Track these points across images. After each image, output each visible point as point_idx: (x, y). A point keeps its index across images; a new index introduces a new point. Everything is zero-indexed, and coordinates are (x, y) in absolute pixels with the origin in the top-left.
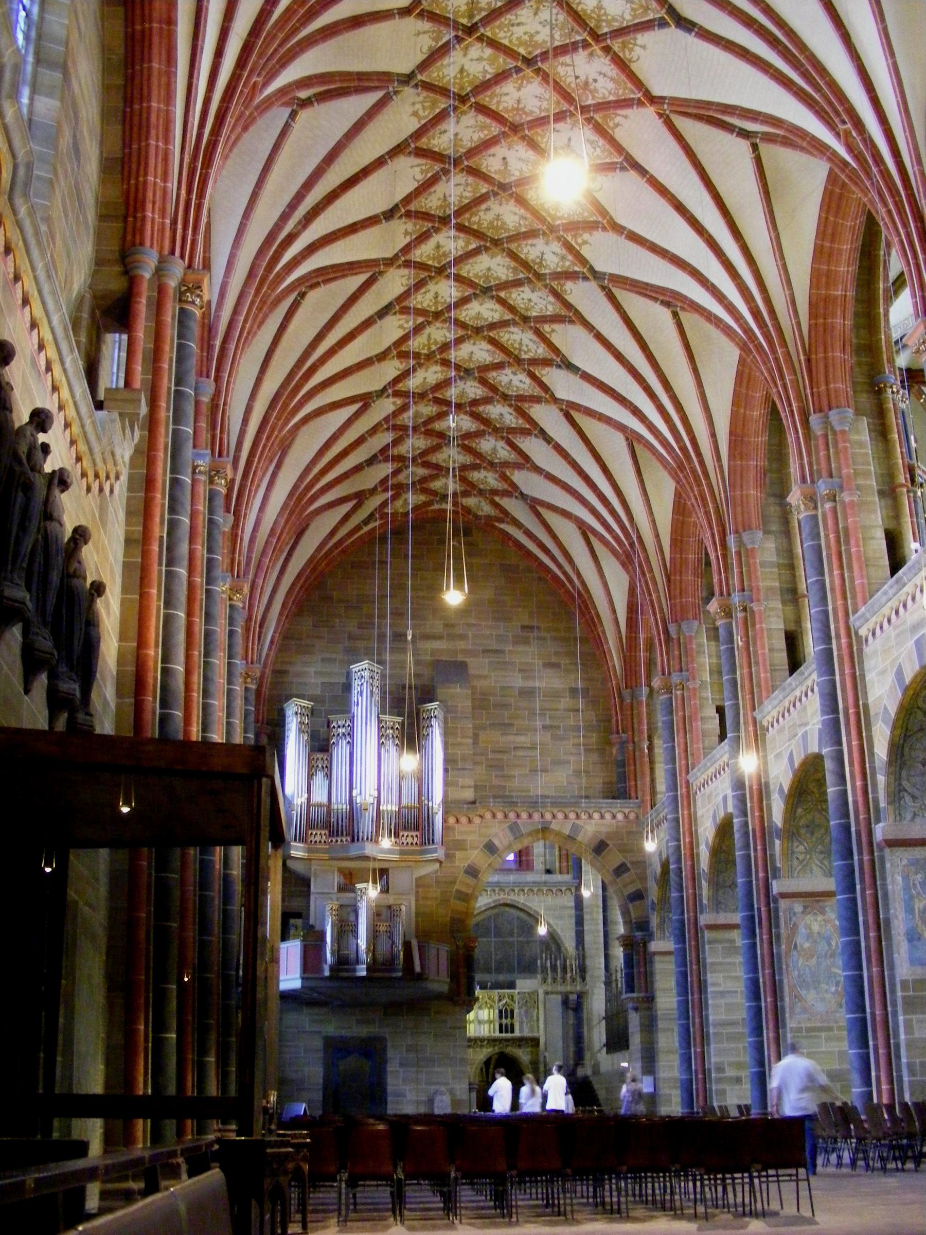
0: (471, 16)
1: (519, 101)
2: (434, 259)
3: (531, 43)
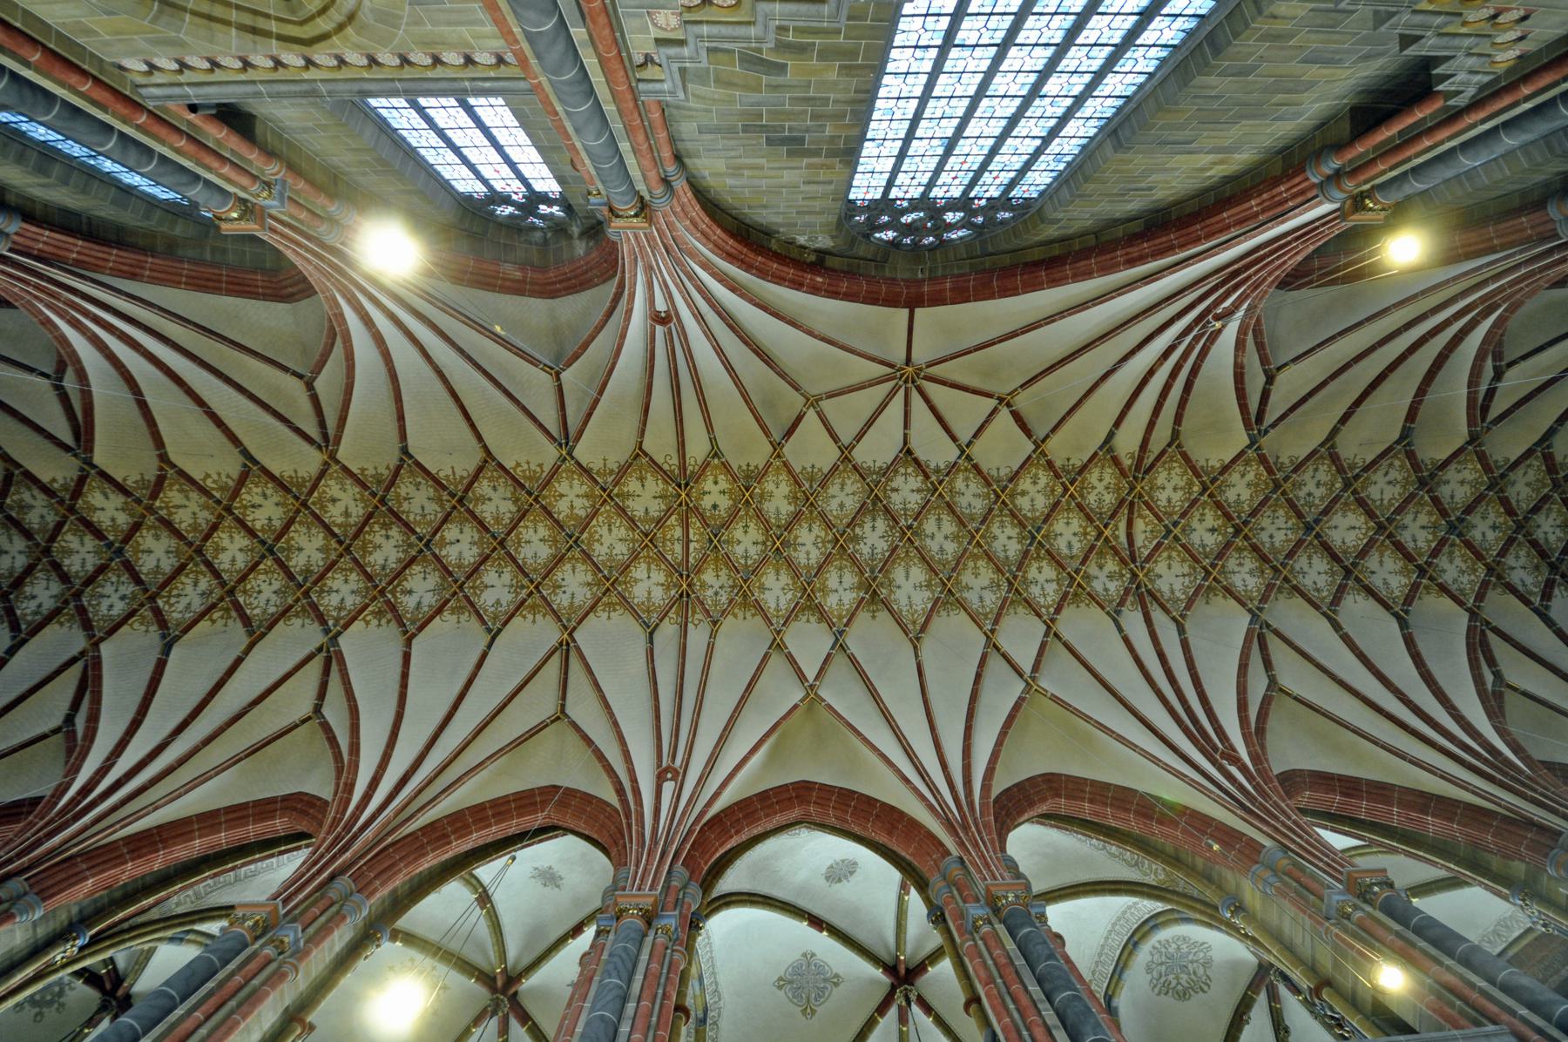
0: (618, 495)
2: (320, 498)
3: (591, 540)
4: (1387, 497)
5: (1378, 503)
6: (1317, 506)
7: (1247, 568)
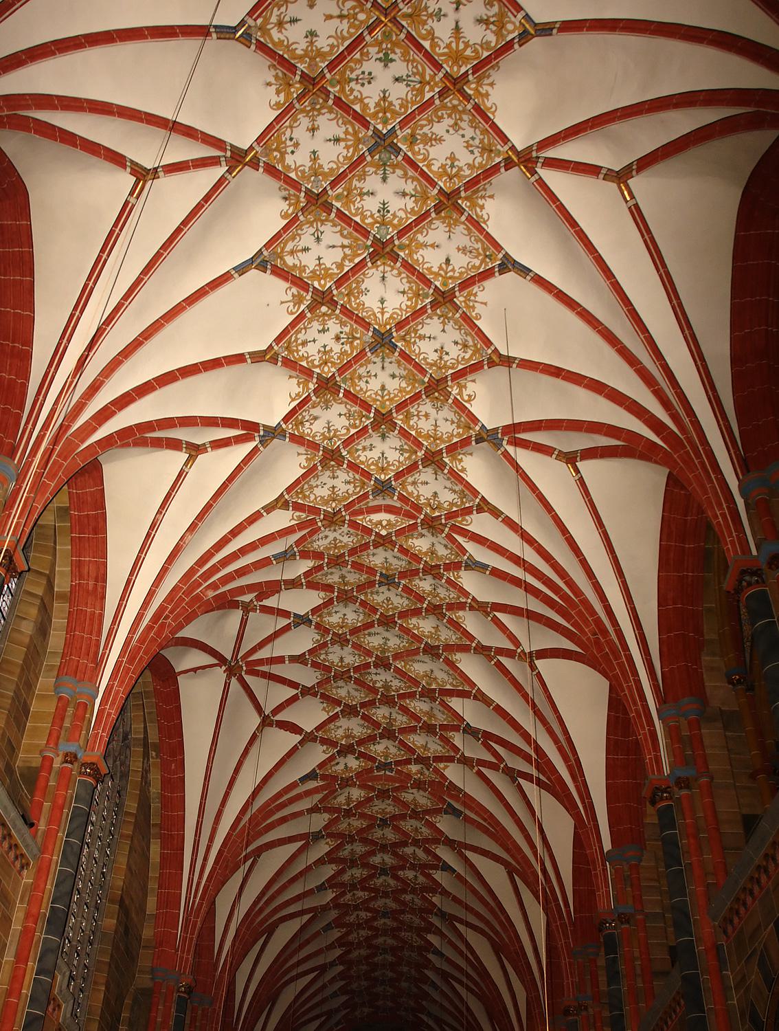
1: (383, 835)
4: (339, 241)
5: (348, 251)
6: (352, 329)
7: (432, 412)
